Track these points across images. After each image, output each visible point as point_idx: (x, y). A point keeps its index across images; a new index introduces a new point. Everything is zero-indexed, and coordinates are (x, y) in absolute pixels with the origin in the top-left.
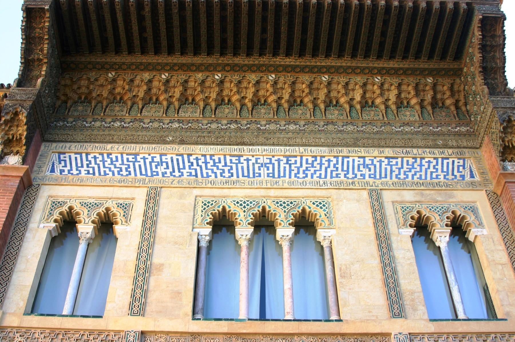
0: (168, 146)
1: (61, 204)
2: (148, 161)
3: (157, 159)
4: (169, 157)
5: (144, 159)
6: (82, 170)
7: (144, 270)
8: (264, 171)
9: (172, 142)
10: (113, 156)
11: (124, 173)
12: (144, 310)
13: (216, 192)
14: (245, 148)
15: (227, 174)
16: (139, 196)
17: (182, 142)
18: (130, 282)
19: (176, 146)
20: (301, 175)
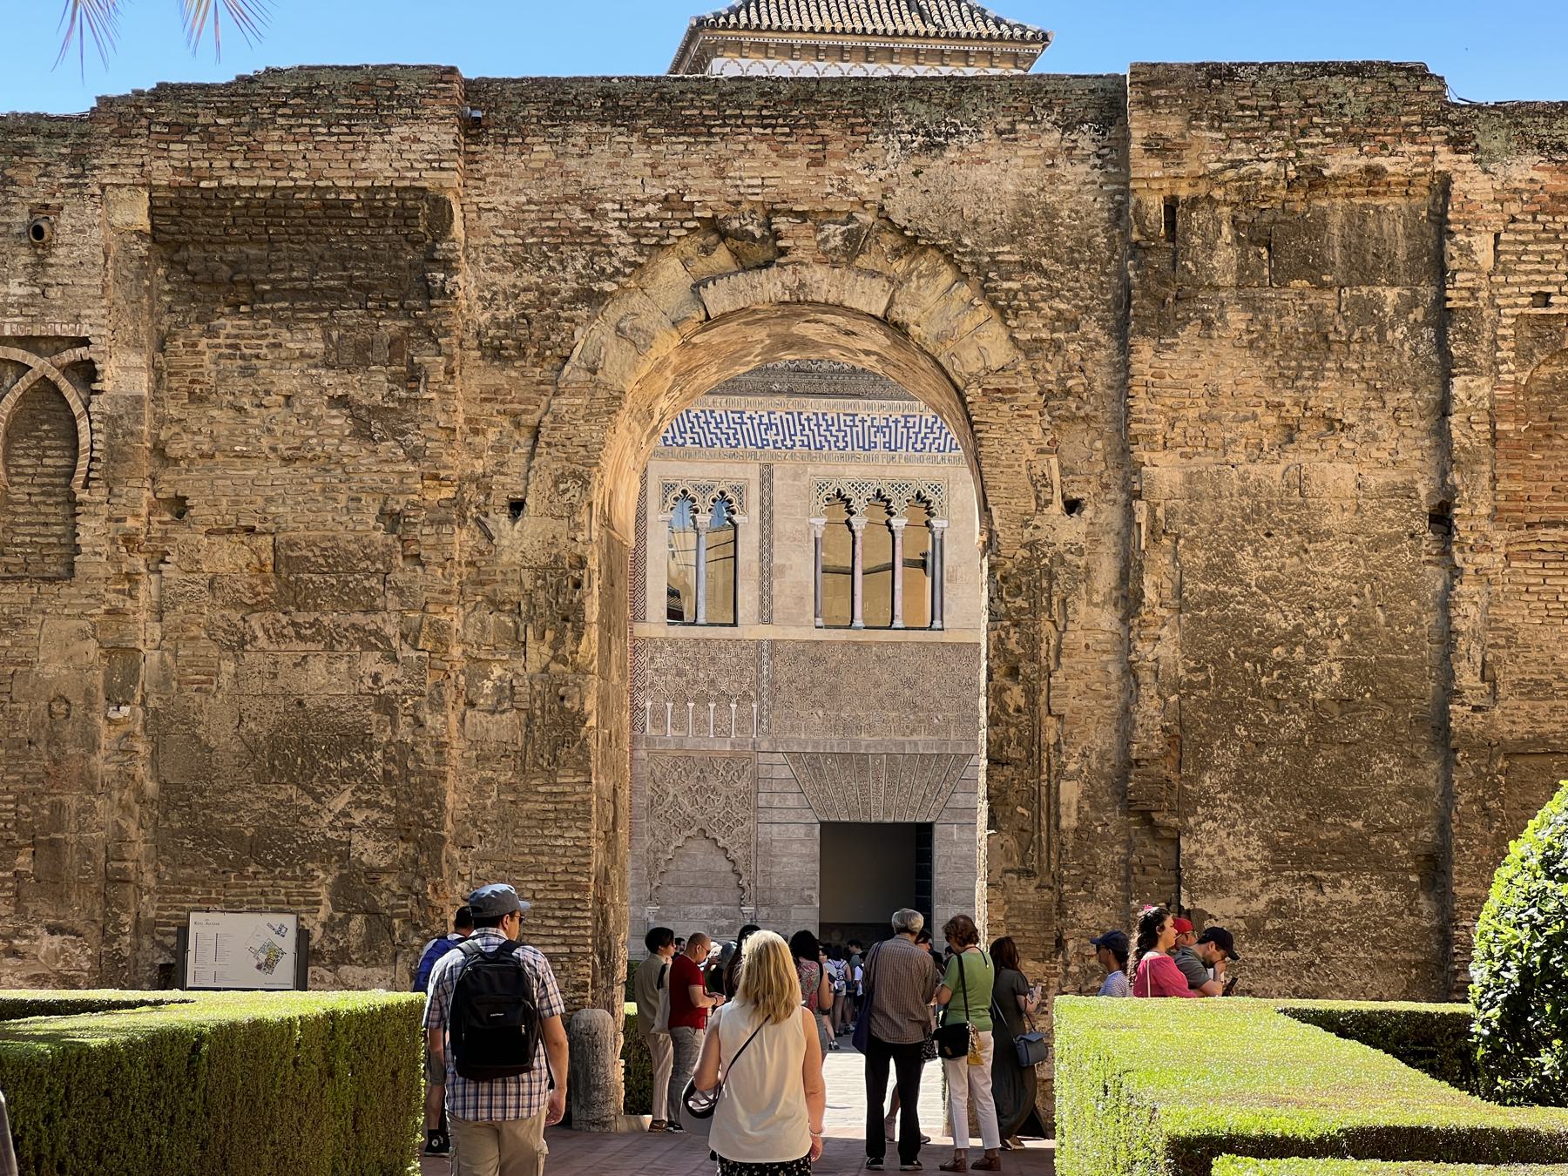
0: (777, 399)
1: (673, 487)
2: (756, 422)
3: (765, 420)
4: (777, 415)
5: (751, 418)
6: (687, 436)
7: (767, 574)
8: (880, 439)
9: (780, 392)
10: (716, 415)
11: (733, 442)
12: (771, 617)
13: (831, 470)
14: (861, 402)
15: (841, 444)
16: (749, 473)
17: (791, 392)
18: (756, 586)
19: (783, 399)
20: (919, 446)
